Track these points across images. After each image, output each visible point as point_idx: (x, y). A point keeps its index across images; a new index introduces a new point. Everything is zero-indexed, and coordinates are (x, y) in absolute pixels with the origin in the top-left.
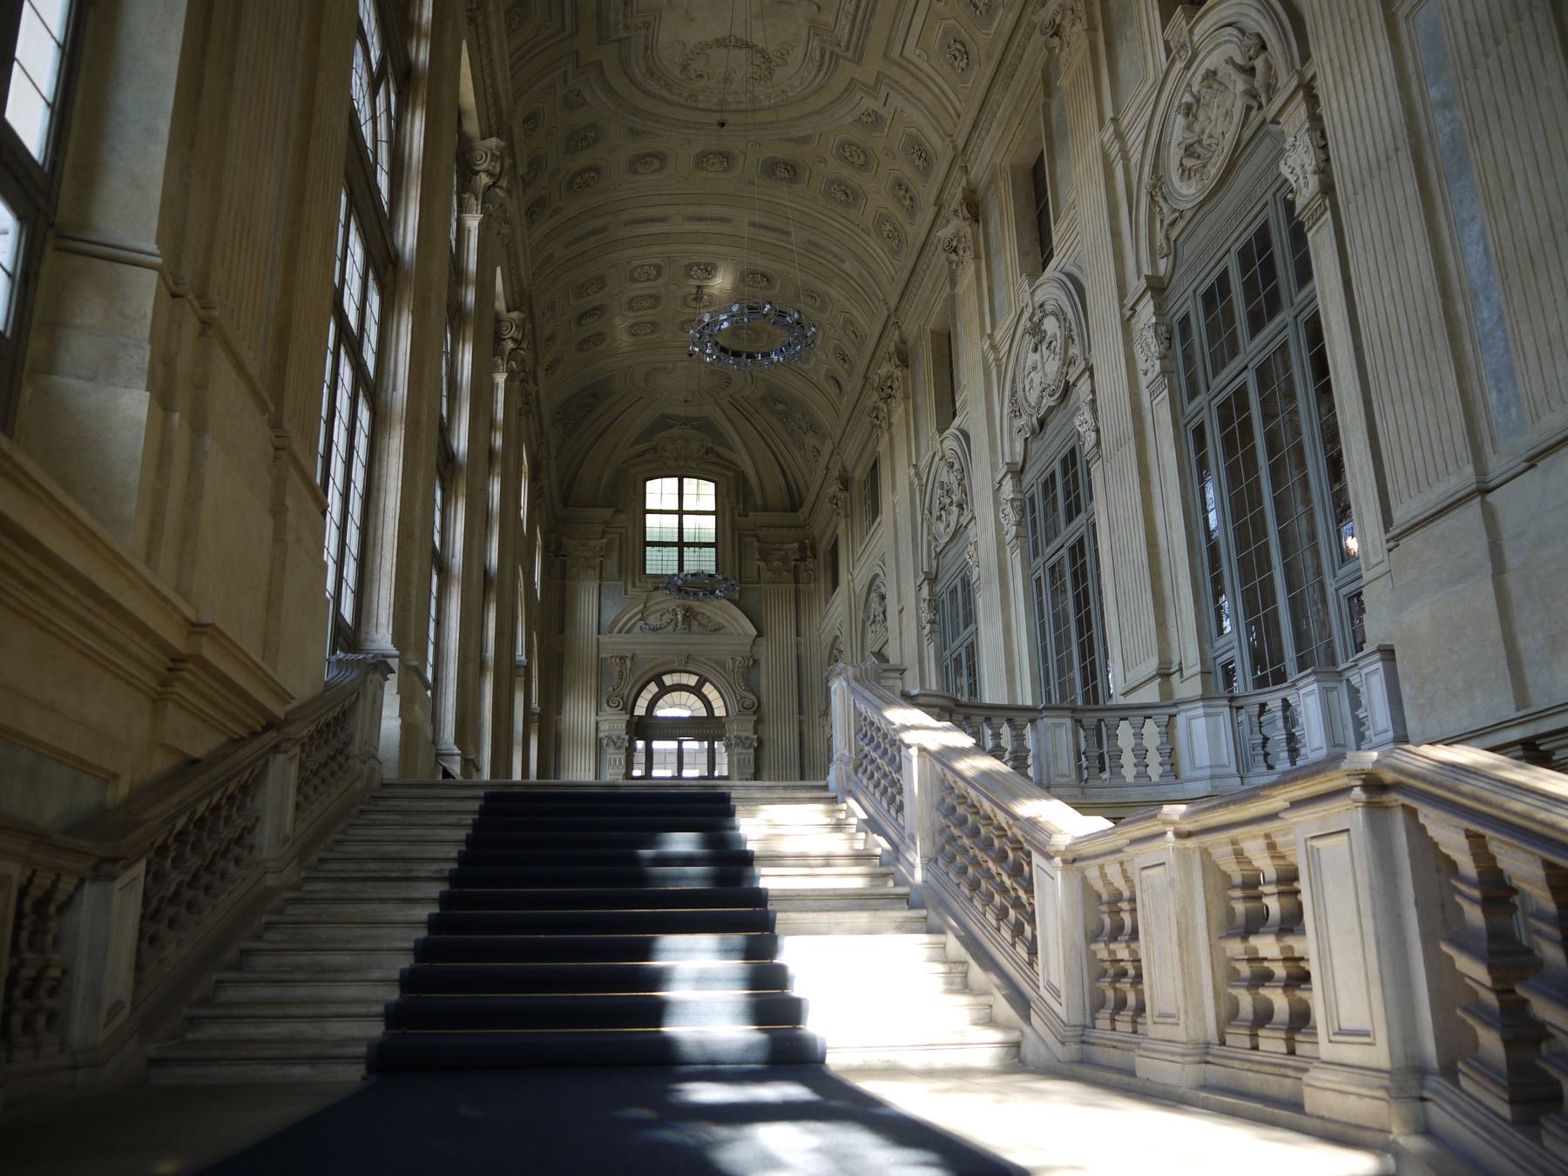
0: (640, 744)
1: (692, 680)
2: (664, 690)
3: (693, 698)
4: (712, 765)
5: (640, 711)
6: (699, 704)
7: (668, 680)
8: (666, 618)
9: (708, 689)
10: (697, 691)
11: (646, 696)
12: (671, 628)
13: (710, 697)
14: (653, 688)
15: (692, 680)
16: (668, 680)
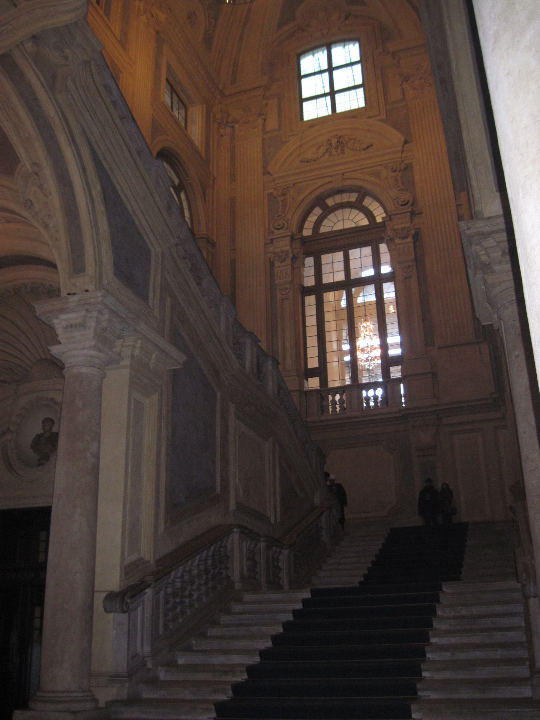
0: (310, 261)
1: (353, 197)
2: (327, 211)
3: (355, 212)
4: (377, 264)
5: (307, 232)
6: (361, 216)
7: (330, 202)
8: (322, 150)
9: (368, 202)
10: (358, 206)
11: (312, 218)
12: (326, 157)
13: (371, 208)
14: (318, 211)
15: (353, 197)
16: (330, 202)
